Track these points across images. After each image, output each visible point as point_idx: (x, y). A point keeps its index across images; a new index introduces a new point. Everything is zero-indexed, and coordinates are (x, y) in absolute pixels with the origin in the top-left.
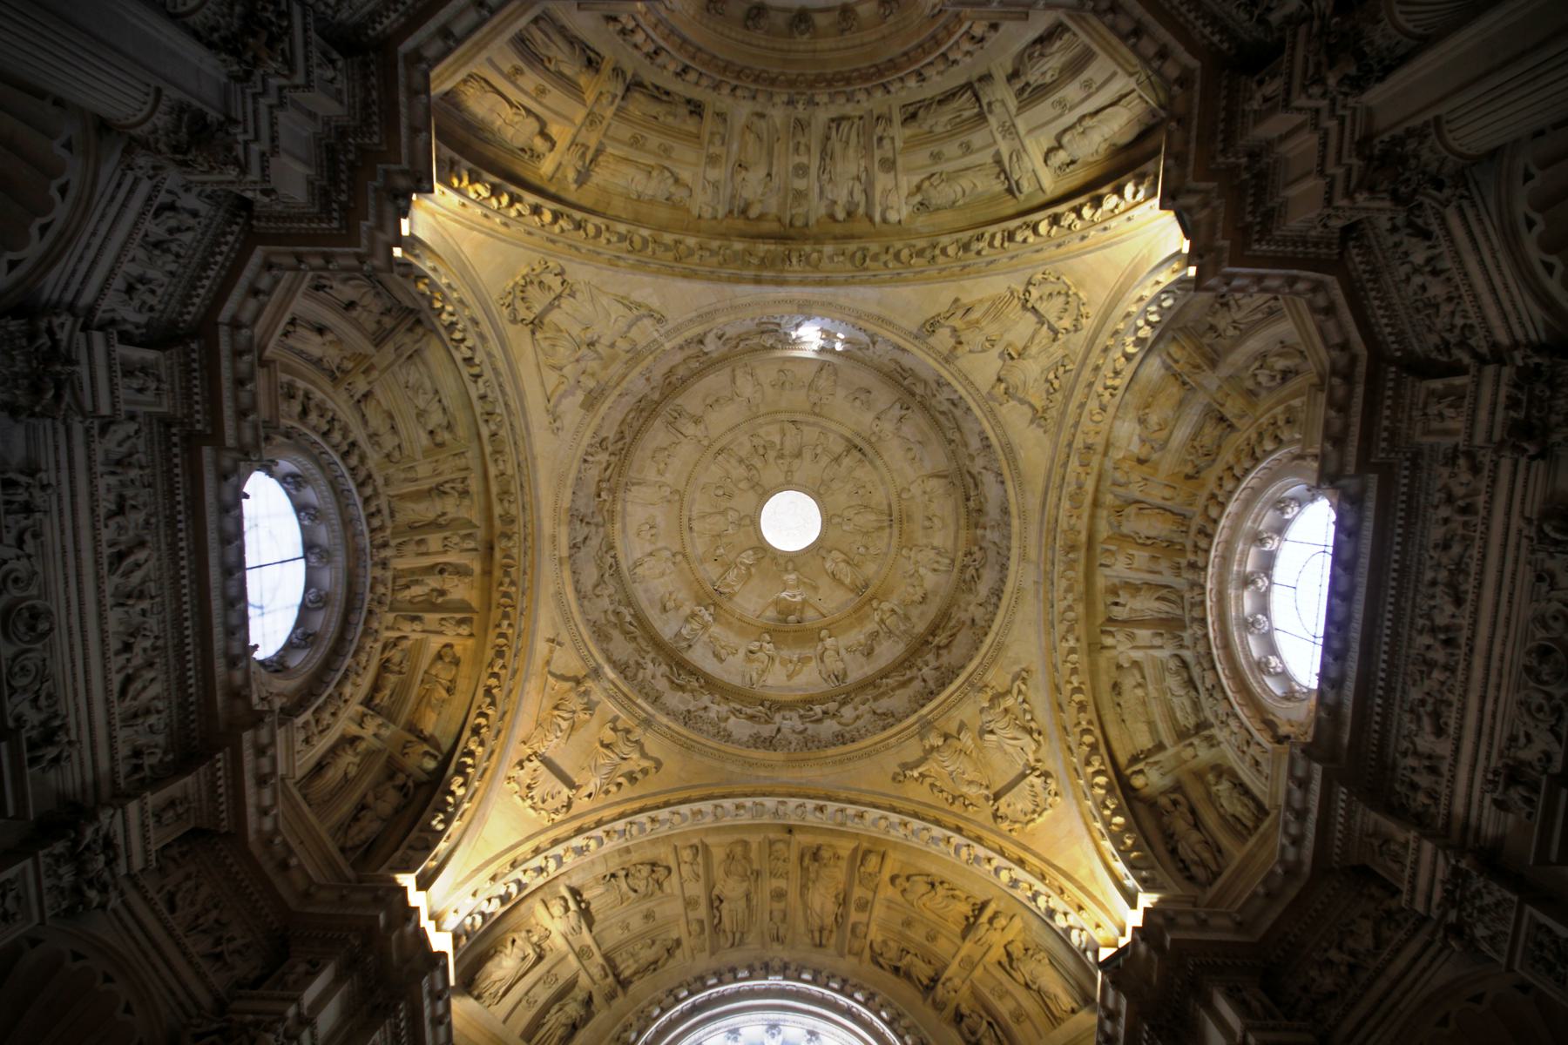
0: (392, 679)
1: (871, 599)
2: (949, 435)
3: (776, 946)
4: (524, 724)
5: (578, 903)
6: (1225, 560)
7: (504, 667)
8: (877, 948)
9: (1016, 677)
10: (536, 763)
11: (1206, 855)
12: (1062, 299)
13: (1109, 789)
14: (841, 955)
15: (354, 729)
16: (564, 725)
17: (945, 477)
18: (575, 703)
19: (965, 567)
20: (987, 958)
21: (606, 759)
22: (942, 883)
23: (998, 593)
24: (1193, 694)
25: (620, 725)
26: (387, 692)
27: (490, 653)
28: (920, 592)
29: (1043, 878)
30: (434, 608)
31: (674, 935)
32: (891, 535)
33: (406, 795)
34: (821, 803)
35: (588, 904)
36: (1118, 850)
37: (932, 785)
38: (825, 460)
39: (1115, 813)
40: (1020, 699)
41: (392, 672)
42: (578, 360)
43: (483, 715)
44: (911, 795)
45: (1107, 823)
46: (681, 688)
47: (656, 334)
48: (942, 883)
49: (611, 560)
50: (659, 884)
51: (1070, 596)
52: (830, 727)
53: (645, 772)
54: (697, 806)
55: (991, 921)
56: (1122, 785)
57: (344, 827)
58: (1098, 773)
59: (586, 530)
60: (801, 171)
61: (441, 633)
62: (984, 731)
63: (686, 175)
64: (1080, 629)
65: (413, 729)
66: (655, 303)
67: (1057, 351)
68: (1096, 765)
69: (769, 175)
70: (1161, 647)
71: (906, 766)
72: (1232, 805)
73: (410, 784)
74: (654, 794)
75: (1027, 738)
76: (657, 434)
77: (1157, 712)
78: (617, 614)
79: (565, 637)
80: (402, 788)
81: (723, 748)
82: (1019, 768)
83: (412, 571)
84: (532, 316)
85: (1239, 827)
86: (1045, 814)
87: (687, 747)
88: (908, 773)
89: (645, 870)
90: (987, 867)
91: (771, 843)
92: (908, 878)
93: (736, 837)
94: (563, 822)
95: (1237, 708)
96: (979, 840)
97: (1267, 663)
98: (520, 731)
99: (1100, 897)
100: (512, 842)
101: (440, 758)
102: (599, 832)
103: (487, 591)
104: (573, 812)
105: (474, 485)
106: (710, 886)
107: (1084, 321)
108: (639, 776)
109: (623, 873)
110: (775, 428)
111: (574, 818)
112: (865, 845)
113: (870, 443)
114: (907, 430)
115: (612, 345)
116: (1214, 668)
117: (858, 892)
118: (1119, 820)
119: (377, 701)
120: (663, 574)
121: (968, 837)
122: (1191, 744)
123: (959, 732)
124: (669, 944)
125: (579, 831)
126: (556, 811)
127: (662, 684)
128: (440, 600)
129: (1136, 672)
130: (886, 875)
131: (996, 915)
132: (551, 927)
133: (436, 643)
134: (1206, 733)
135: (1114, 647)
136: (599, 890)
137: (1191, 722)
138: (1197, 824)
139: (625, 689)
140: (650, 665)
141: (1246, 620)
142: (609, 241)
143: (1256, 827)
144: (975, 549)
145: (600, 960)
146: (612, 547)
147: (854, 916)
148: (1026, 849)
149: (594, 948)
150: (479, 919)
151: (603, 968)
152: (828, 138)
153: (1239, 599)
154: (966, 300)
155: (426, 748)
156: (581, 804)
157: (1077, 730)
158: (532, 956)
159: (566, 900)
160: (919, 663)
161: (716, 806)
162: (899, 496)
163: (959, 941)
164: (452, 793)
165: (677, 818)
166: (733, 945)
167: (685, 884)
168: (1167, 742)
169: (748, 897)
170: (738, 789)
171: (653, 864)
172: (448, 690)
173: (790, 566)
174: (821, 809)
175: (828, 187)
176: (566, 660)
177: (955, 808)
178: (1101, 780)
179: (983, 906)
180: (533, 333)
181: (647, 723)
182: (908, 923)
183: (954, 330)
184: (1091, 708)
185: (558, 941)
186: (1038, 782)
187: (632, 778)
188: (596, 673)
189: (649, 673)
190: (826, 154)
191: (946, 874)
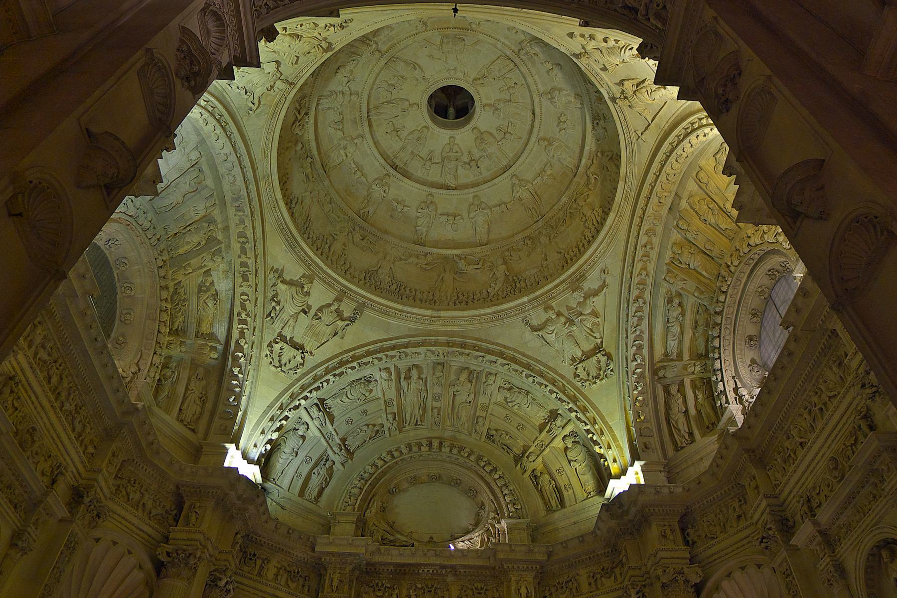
12: (283, 362)
28: (339, 76)
42: (581, 314)
60: (437, 398)
66: (528, 334)
67: (277, 326)
84: (598, 355)
107: (268, 353)
110: (462, 180)
115: (559, 314)
120: (560, 90)
152: (423, 415)
162: (362, 137)
175: (422, 387)
183: (343, 320)
190: (423, 407)
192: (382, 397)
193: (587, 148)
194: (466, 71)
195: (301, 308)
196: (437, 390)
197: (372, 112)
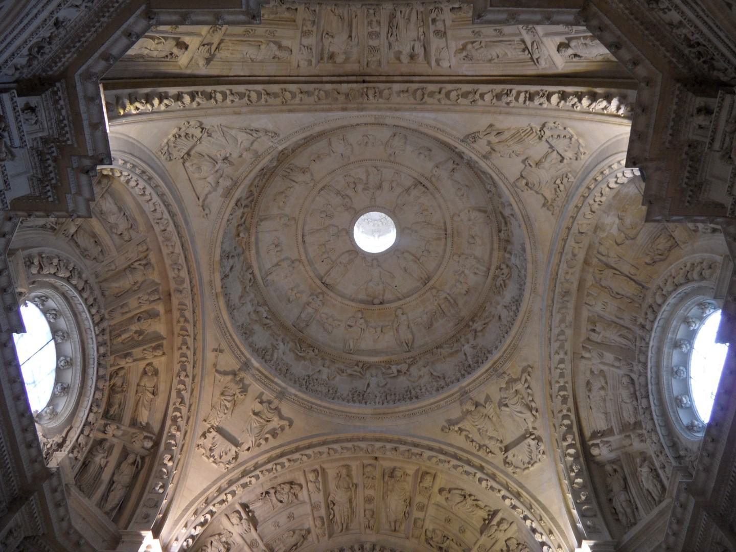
0: (118, 397)
1: (431, 288)
2: (488, 187)
3: (368, 531)
4: (204, 409)
5: (247, 513)
6: (664, 330)
7: (187, 376)
8: (429, 534)
9: (524, 371)
10: (214, 433)
11: (628, 511)
13: (576, 457)
14: (408, 538)
15: (101, 436)
16: (228, 405)
17: (485, 212)
18: (235, 389)
19: (496, 277)
21: (255, 423)
22: (470, 495)
23: (517, 302)
24: (635, 403)
25: (264, 398)
26: (117, 406)
27: (177, 367)
28: (465, 287)
29: (530, 508)
30: (139, 344)
31: (306, 527)
32: (446, 245)
33: (137, 467)
34: (396, 445)
35: (254, 512)
36: (576, 503)
37: (467, 437)
38: (398, 191)
39: (577, 476)
40: (526, 385)
41: (117, 393)
42: (217, 171)
43: (177, 409)
44: (453, 442)
45: (572, 483)
46: (303, 358)
47: (271, 144)
48: (470, 495)
49: (249, 276)
50: (296, 495)
51: (563, 326)
52: (403, 381)
53: (282, 428)
54: (317, 450)
55: (499, 524)
56: (585, 454)
57: (105, 497)
58: (570, 446)
59: (231, 261)
60: (375, 35)
61: (144, 359)
62: (503, 404)
63: (286, 43)
64: (568, 346)
65: (134, 423)
66: (270, 127)
68: (570, 441)
69: (350, 36)
70: (618, 368)
71: (451, 423)
72: (648, 484)
73: (139, 459)
74: (289, 443)
75: (529, 414)
76: (278, 184)
77: (611, 409)
78: (256, 312)
79: (224, 346)
80: (134, 463)
81: (332, 406)
82: (522, 432)
83: (121, 324)
85: (650, 498)
86: (536, 465)
87: (309, 408)
88: (452, 427)
89: (287, 488)
90: (498, 495)
91: (364, 466)
92: (449, 491)
93: (342, 463)
94: (234, 469)
95: (658, 428)
96: (493, 477)
97: (681, 401)
98: (202, 415)
99: (562, 527)
100: (205, 486)
101: (154, 437)
102: (257, 472)
103: (170, 323)
104: (240, 460)
105: (153, 258)
106: (327, 495)
108: (279, 431)
109: (272, 491)
111: (240, 465)
112: (424, 469)
113: (431, 182)
114: (458, 176)
116: (647, 397)
117: (418, 499)
118: (579, 480)
119: (111, 412)
121: (487, 474)
122: (629, 436)
123: (486, 403)
124: (304, 533)
125: (244, 474)
126: (229, 463)
127: (289, 358)
128: (141, 338)
129: (602, 379)
130: (436, 489)
131: (502, 520)
132: (232, 531)
133: (142, 365)
134: (640, 432)
135: (589, 359)
136: (259, 504)
137: (632, 421)
138: (626, 488)
139: (266, 373)
140: (281, 344)
141: (672, 369)
142: (232, 101)
143: (660, 502)
144: (503, 266)
145: (264, 548)
146: (250, 267)
147: (417, 514)
148: (523, 487)
149: (259, 541)
150: (190, 541)
153: (670, 355)
154: (499, 126)
155: (146, 434)
156: (244, 455)
157: (560, 415)
160: (463, 340)
161: (329, 449)
162: (452, 218)
163: (478, 535)
164: (166, 465)
165: (305, 458)
166: (342, 530)
167: (310, 494)
168: (616, 430)
169: (350, 501)
170: (342, 436)
171: (291, 483)
172: (153, 394)
173: (375, 263)
174: (396, 449)
176: (228, 361)
178: (572, 451)
179: (495, 513)
180: (184, 163)
181: (282, 395)
182: (448, 520)
184: (570, 401)
186: (533, 443)
187: (274, 433)
188: (246, 365)
189: (281, 351)
191: (473, 492)
192: (449, 42)
193: (253, 252)
194: (364, 265)
195: (533, 169)
196: (374, 43)
197: (443, 236)
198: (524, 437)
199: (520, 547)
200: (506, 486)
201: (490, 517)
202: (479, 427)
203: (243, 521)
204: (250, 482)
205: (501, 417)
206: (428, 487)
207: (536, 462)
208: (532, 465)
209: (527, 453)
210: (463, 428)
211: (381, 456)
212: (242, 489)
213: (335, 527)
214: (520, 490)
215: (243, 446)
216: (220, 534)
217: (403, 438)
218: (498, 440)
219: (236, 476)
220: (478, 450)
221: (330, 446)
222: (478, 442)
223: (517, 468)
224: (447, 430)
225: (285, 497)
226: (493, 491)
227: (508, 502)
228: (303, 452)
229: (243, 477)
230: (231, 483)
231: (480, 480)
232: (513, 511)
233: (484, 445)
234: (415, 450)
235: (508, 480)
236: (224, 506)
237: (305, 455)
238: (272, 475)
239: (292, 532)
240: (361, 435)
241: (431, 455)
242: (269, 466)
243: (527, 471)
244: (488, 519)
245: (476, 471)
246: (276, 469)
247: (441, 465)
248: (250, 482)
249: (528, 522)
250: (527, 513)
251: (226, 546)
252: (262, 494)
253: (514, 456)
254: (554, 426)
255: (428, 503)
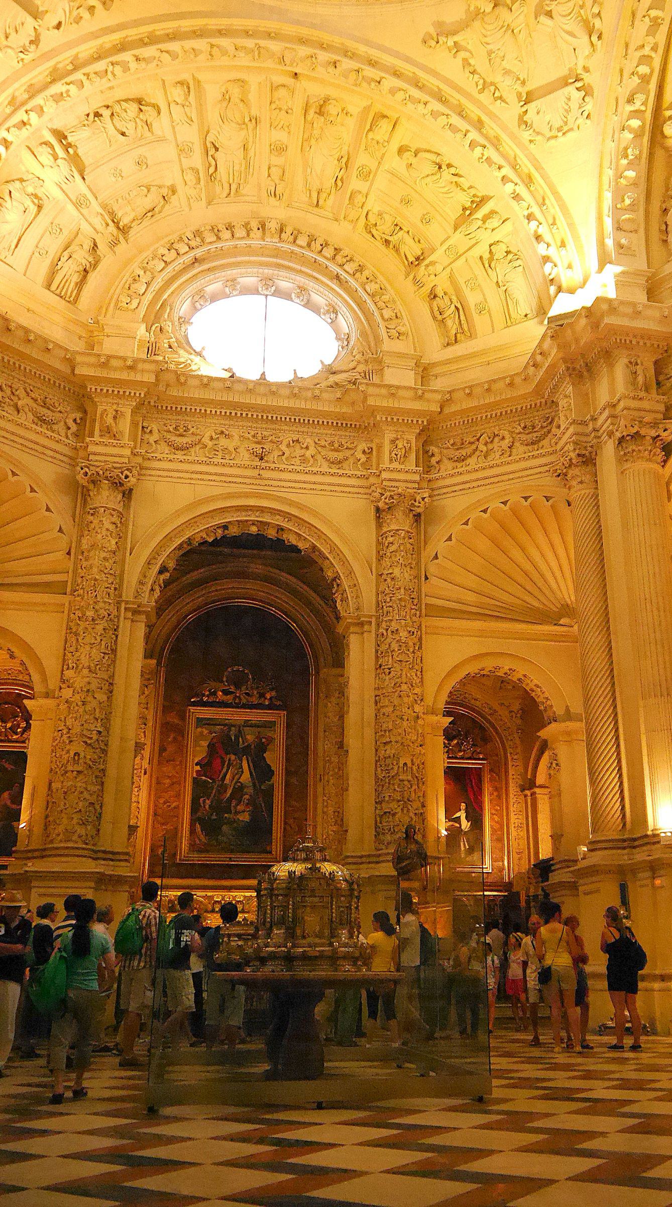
20: (470, 253)
54: (189, 44)
55: (485, 219)
71: (443, 31)
74: (136, 23)
88: (442, 39)
96: (496, 143)
109: (106, 113)
121: (486, 137)
136: (85, 133)
145: (100, 210)
148: (538, 167)
149: (90, 196)
151: (104, 220)
158: (33, 209)
159: (53, 148)
165: (166, 57)
177: (485, 98)
185: (51, 189)
198: (564, 82)
199: (510, 257)
200: (512, 159)
201: (474, 206)
202: (490, 47)
203: (59, 161)
204: (68, 91)
205: (533, 34)
206: (381, 141)
207: (571, 129)
208: (564, 134)
209: (561, 111)
210: (463, 43)
211: (306, 73)
212: (54, 105)
213: (218, 189)
214: (533, 170)
215: (47, 17)
216: (21, 180)
217: (351, 44)
218: (518, 79)
219: (40, 78)
220: (481, 91)
221: (215, 41)
222: (483, 76)
223: (538, 133)
224: (433, 43)
225: (131, 125)
226: (490, 166)
227: (509, 187)
228: (163, 46)
229: (53, 81)
230: (33, 91)
231: (472, 145)
232: (514, 203)
233: (492, 84)
234: (369, 72)
235: (518, 152)
236: (25, 132)
237: (167, 52)
238: (104, 83)
239: (146, 190)
240: (272, 25)
241: (396, 85)
242: (101, 66)
243: (553, 142)
244: (470, 208)
245: (469, 128)
246: (112, 73)
247: (410, 106)
248: (68, 91)
249: (534, 224)
250: (535, 210)
251: (36, 201)
252: (88, 115)
253: (538, 113)
254: (621, 71)
255: (378, 167)
